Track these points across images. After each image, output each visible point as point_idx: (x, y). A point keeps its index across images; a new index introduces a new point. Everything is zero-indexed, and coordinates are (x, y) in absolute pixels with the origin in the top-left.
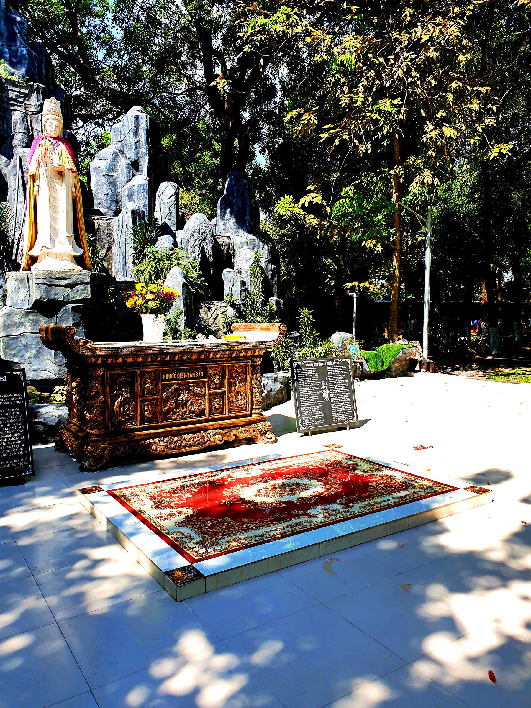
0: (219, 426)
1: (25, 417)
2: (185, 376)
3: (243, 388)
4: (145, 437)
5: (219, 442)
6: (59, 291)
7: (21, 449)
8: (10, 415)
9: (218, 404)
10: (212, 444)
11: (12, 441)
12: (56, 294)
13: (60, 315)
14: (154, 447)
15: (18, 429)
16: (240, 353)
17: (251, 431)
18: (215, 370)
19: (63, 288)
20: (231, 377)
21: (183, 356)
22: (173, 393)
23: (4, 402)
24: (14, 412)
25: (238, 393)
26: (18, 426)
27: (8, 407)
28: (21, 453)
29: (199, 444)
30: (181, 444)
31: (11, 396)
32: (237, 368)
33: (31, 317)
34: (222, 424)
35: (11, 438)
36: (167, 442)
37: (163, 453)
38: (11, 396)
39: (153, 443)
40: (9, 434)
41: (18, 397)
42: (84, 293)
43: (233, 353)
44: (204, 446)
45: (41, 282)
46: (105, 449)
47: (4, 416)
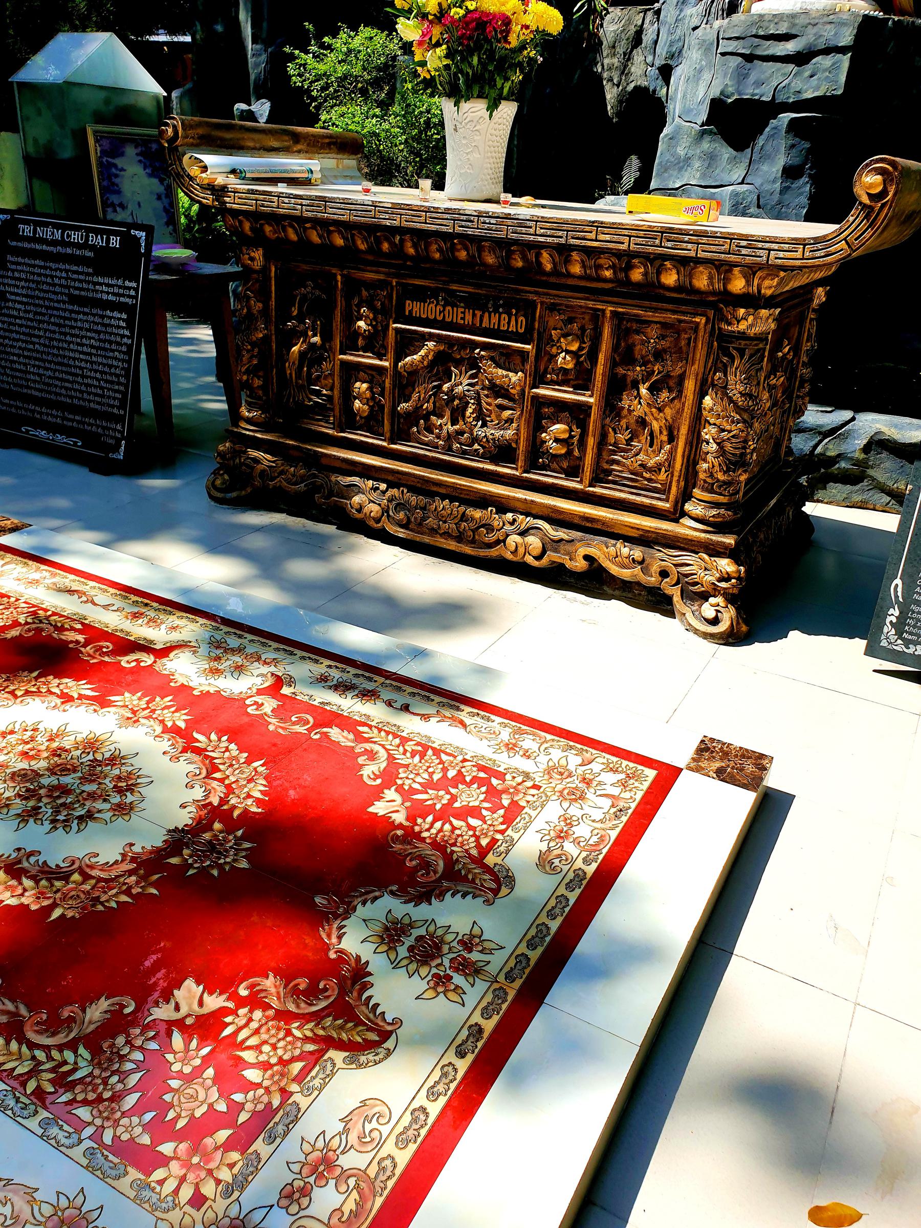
0: (546, 512)
1: (131, 337)
2: (469, 318)
3: (668, 411)
4: (344, 466)
5: (529, 560)
6: (767, 74)
7: (116, 403)
8: (112, 326)
9: (557, 440)
10: (509, 556)
11: (107, 381)
12: (759, 83)
13: (761, 141)
14: (357, 499)
15: (119, 360)
16: (659, 273)
17: (655, 568)
18: (571, 320)
19: (779, 65)
20: (624, 355)
21: (453, 248)
22: (432, 364)
23: (108, 293)
24: (119, 319)
25: (642, 422)
26: (120, 352)
27: (113, 306)
28: (115, 411)
29: (472, 542)
30: (424, 519)
31: (120, 282)
32: (653, 332)
33: (706, 145)
34: (555, 510)
35: (106, 373)
36: (390, 500)
37: (372, 523)
38: (120, 282)
39: (360, 491)
40: (104, 365)
41: (129, 288)
42: (828, 78)
43: (630, 267)
44: (483, 553)
45: (729, 50)
46: (256, 461)
47: (104, 325)
